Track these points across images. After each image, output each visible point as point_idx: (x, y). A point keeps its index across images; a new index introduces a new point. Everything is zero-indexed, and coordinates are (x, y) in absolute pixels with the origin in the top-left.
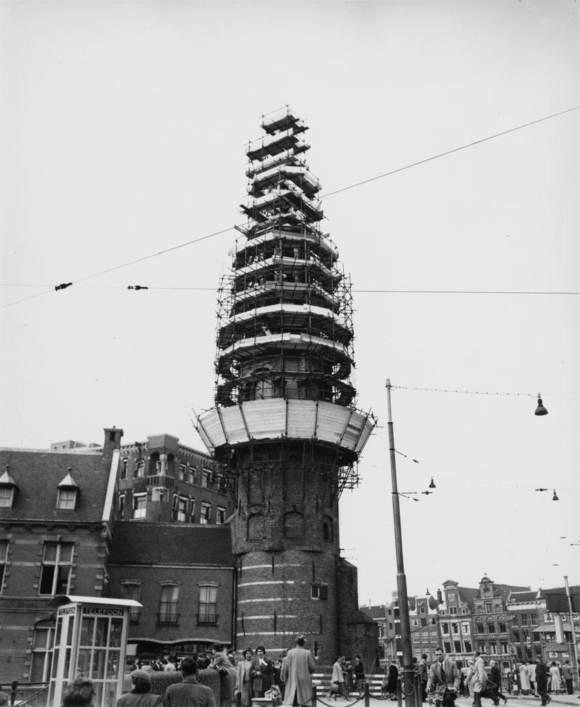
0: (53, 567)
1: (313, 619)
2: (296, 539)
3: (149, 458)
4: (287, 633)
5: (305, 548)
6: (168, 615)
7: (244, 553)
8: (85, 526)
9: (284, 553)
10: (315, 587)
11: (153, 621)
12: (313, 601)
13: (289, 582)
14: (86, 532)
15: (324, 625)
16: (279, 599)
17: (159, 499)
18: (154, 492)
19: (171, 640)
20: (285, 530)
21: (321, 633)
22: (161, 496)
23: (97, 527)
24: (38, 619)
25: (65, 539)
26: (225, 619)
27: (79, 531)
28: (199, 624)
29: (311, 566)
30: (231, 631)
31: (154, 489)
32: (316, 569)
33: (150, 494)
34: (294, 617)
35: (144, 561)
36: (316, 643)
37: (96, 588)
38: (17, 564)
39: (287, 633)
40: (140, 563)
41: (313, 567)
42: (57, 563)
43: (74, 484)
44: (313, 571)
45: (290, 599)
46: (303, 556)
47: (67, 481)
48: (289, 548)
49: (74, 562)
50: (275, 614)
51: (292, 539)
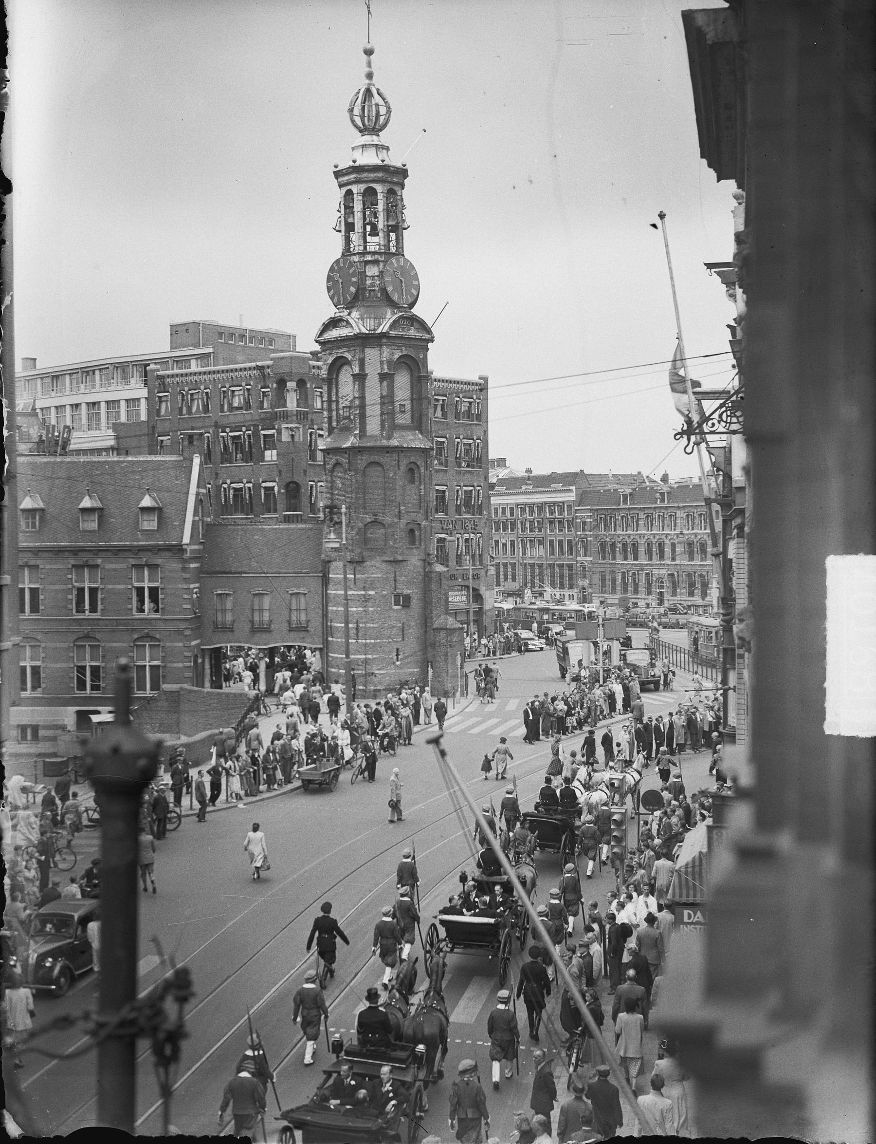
0: (144, 588)
1: (394, 627)
2: (377, 549)
3: (275, 385)
4: (368, 641)
5: (387, 558)
6: (261, 622)
7: (329, 562)
8: (169, 548)
9: (365, 564)
10: (397, 596)
11: (247, 627)
12: (394, 610)
13: (370, 593)
14: (168, 554)
15: (406, 632)
16: (361, 609)
17: (290, 440)
18: (283, 431)
19: (265, 645)
20: (366, 541)
21: (403, 640)
22: (293, 436)
23: (179, 549)
24: (136, 636)
25: (150, 562)
26: (315, 625)
27: (163, 554)
28: (291, 630)
29: (393, 576)
30: (321, 634)
31: (284, 426)
32: (398, 578)
33: (279, 432)
34: (375, 626)
35: (233, 570)
36: (398, 650)
37: (185, 606)
38: (110, 587)
39: (368, 641)
40: (230, 573)
41: (395, 576)
42: (146, 584)
43: (155, 505)
44: (395, 581)
45: (371, 609)
46: (384, 566)
47: (147, 502)
48: (371, 558)
49: (161, 583)
50: (357, 623)
51: (372, 549)
